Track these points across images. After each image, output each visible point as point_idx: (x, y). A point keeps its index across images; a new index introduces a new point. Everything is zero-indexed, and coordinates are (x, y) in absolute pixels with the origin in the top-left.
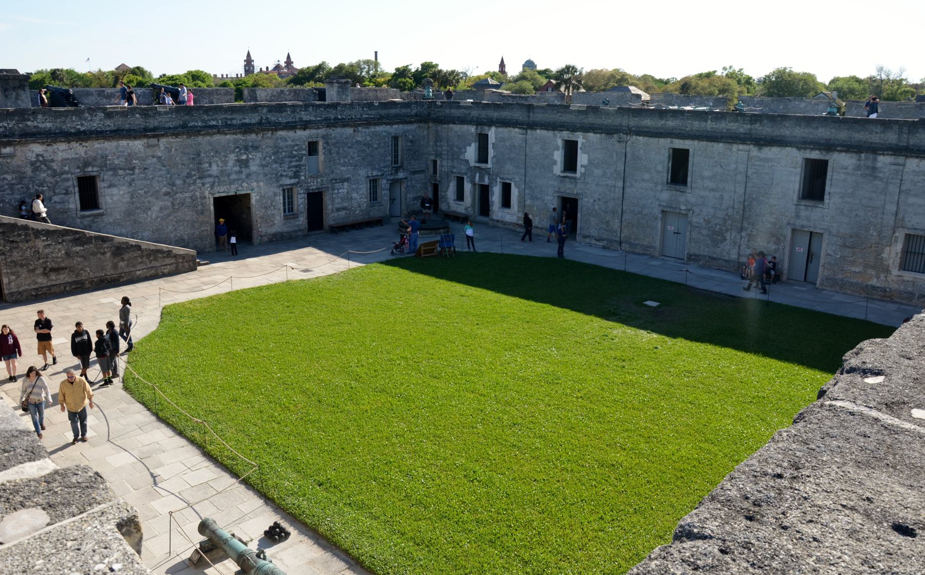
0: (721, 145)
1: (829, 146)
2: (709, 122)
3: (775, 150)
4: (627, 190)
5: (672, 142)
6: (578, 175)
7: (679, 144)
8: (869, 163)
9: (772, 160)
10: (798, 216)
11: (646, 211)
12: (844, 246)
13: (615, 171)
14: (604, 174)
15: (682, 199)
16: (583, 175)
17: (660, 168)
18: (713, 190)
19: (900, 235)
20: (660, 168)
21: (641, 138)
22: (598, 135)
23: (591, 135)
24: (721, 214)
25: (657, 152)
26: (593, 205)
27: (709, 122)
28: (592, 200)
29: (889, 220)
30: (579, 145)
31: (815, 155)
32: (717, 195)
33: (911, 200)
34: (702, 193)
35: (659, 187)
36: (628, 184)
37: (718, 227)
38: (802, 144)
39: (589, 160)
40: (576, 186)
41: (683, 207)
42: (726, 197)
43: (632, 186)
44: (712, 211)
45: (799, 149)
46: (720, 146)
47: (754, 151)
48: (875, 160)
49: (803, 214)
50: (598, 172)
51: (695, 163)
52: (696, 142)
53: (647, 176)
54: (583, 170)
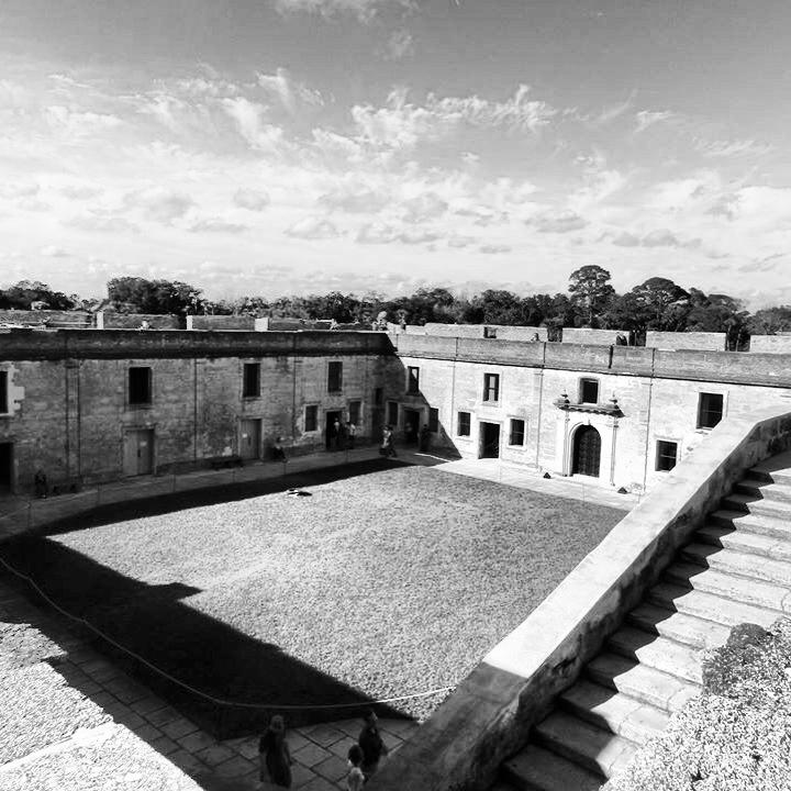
0: (180, 360)
1: (260, 354)
2: (163, 340)
3: (224, 359)
4: (83, 419)
5: (131, 362)
6: (11, 413)
7: (139, 363)
8: (283, 363)
9: (221, 369)
10: (244, 410)
11: (108, 437)
12: (275, 424)
13: (67, 400)
14: (50, 406)
15: (148, 416)
16: (19, 412)
17: (120, 389)
18: (176, 402)
19: (304, 408)
20: (120, 389)
21: (96, 361)
22: (38, 363)
23: (27, 364)
24: (184, 422)
25: (115, 374)
26: (37, 445)
27: (163, 340)
28: (33, 440)
29: (298, 400)
30: (10, 377)
31: (251, 361)
32: (181, 405)
33: (307, 384)
34: (166, 406)
35: (121, 409)
36: (83, 412)
37: (183, 434)
38: (240, 353)
39: (26, 394)
40: (7, 427)
41: (148, 424)
42: (188, 405)
43: (88, 413)
44: (176, 420)
45: (240, 357)
46: (179, 362)
47: (208, 363)
48: (286, 361)
49: (247, 408)
50: (41, 405)
51: (157, 379)
52: (157, 360)
53: (105, 400)
54: (18, 406)
